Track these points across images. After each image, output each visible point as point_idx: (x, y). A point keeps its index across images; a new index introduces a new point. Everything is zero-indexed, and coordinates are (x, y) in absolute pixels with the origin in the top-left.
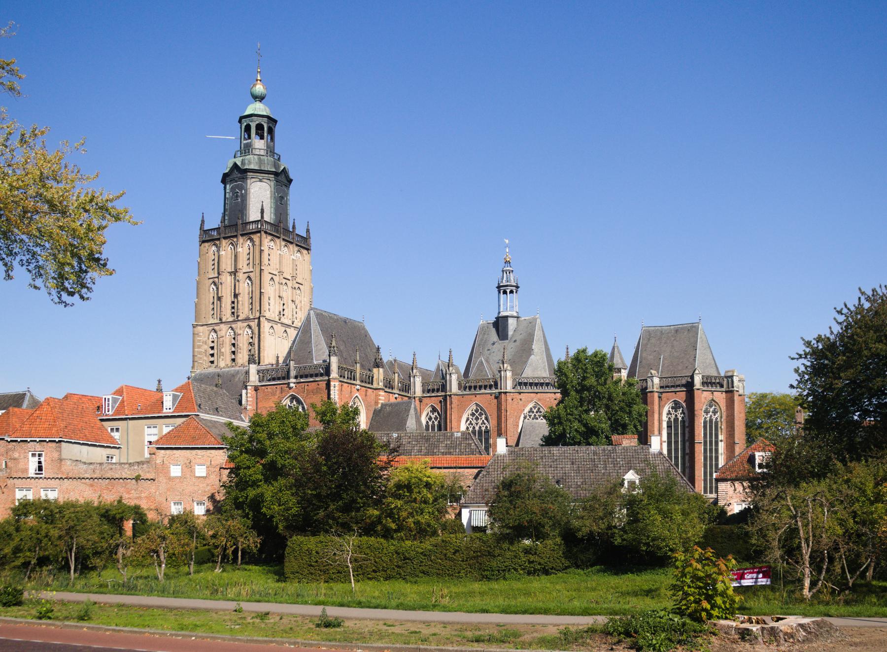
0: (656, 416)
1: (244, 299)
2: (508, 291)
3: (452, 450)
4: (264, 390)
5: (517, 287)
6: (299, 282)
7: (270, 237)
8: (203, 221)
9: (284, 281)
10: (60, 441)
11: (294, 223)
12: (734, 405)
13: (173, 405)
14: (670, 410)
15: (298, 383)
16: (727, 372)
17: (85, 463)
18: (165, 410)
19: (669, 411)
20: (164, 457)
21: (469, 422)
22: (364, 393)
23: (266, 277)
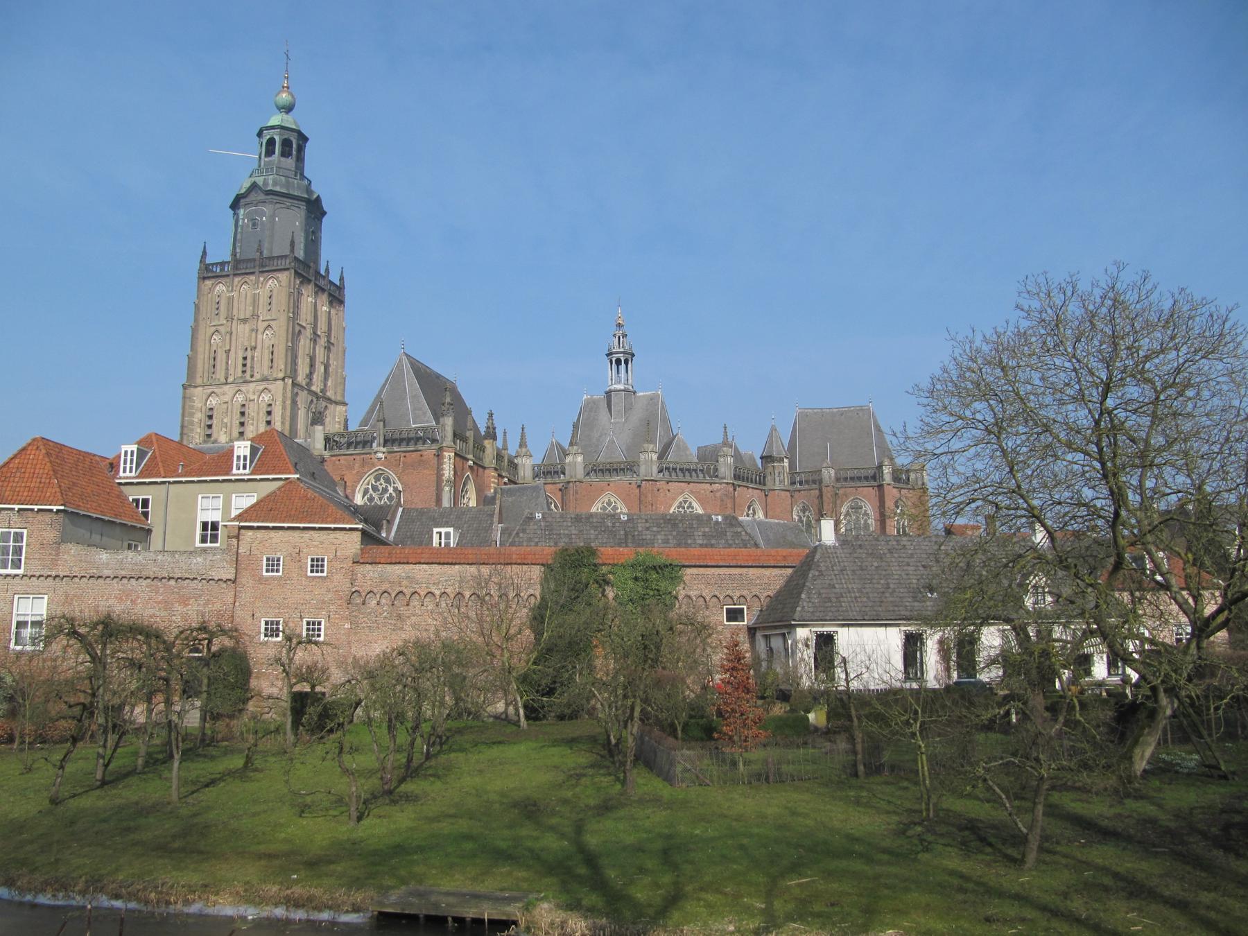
4: (334, 462)
5: (633, 355)
8: (204, 253)
11: (328, 265)
15: (389, 452)
18: (235, 471)
20: (252, 543)
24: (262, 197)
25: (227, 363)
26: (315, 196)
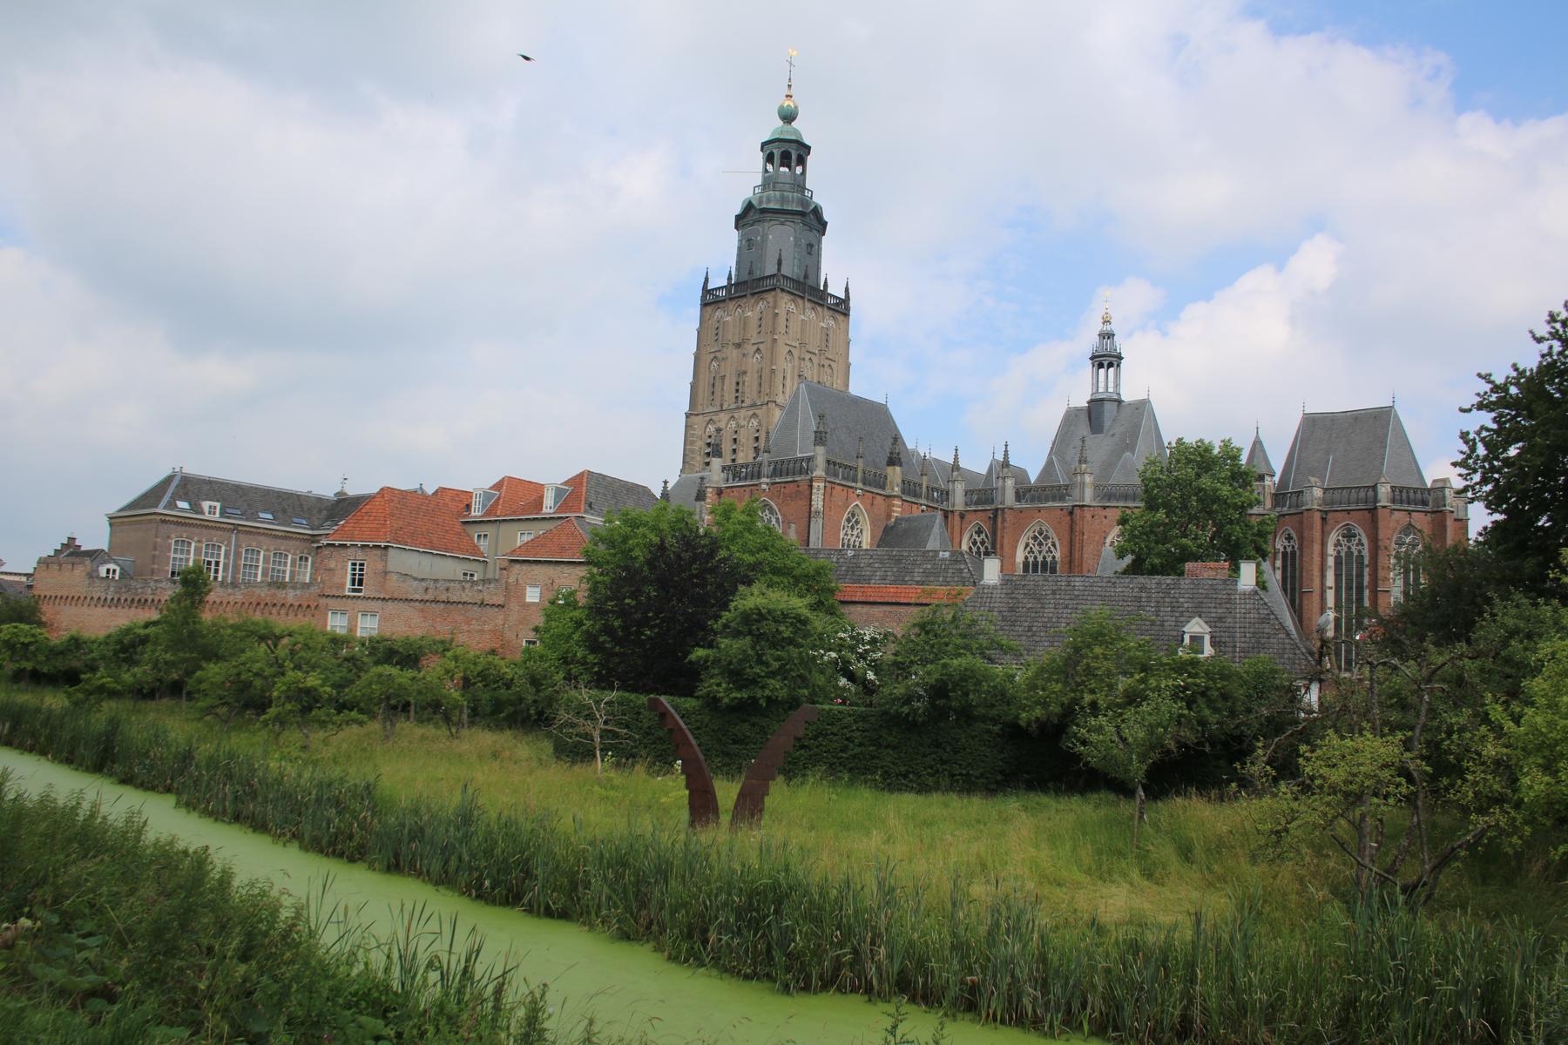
0: (1317, 548)
1: (750, 380)
2: (1106, 364)
3: (931, 579)
6: (811, 350)
7: (786, 297)
8: (707, 280)
9: (808, 356)
10: (387, 547)
12: (1446, 531)
13: (555, 504)
14: (1340, 538)
15: (773, 484)
16: (1434, 481)
17: (415, 579)
18: (544, 510)
19: (1338, 540)
21: (1028, 549)
22: (869, 502)
23: (782, 350)
24: (757, 216)
25: (722, 389)
26: (812, 208)
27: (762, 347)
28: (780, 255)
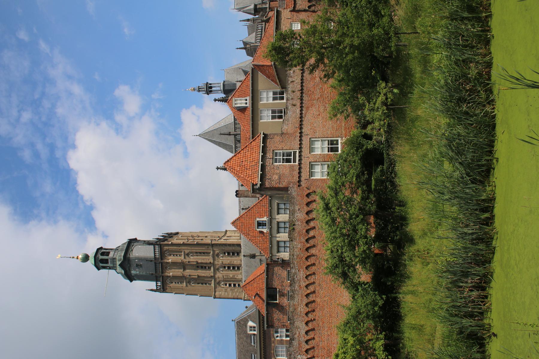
1: (201, 259)
8: (152, 290)
27: (187, 252)
28: (149, 290)
